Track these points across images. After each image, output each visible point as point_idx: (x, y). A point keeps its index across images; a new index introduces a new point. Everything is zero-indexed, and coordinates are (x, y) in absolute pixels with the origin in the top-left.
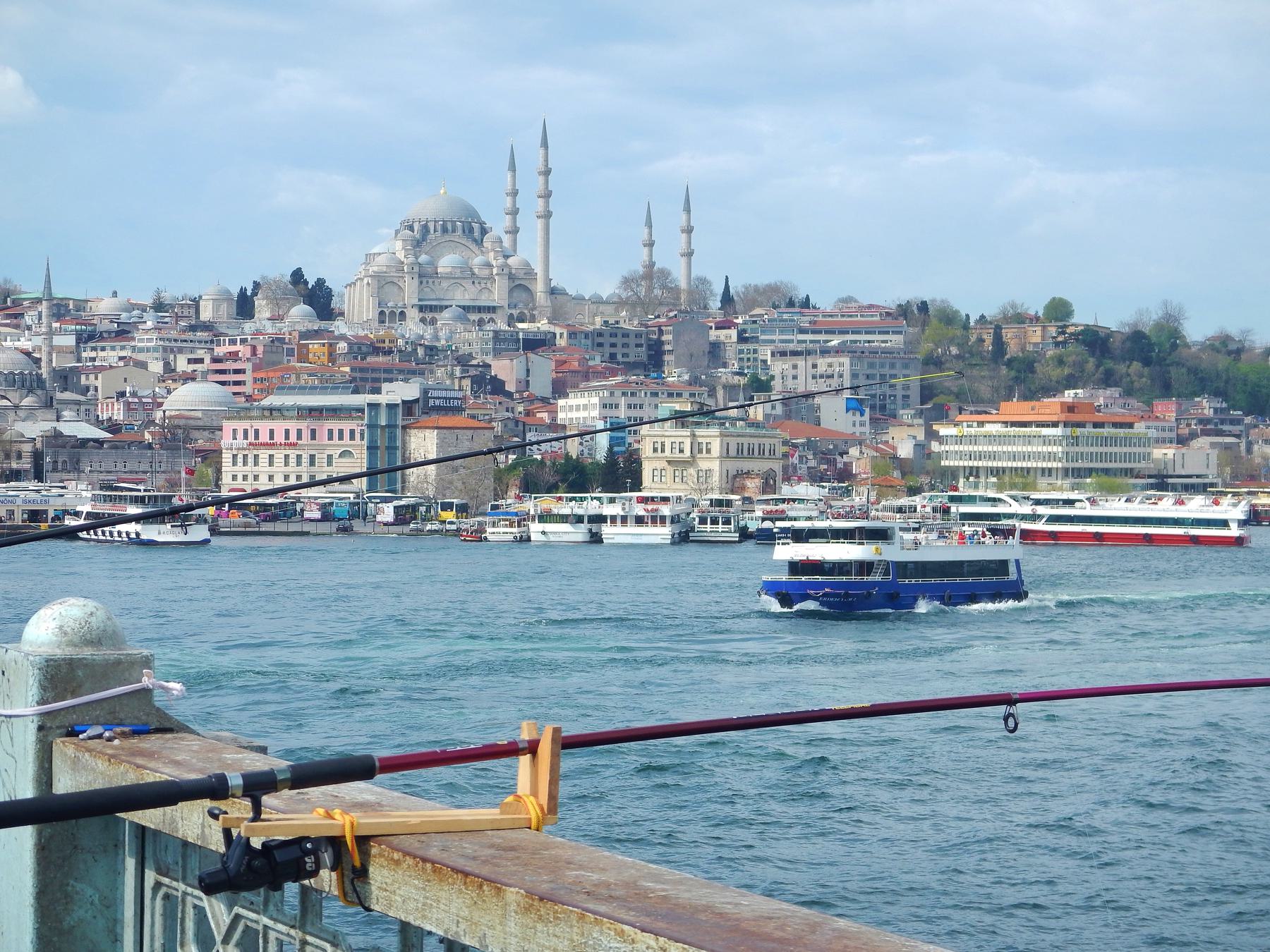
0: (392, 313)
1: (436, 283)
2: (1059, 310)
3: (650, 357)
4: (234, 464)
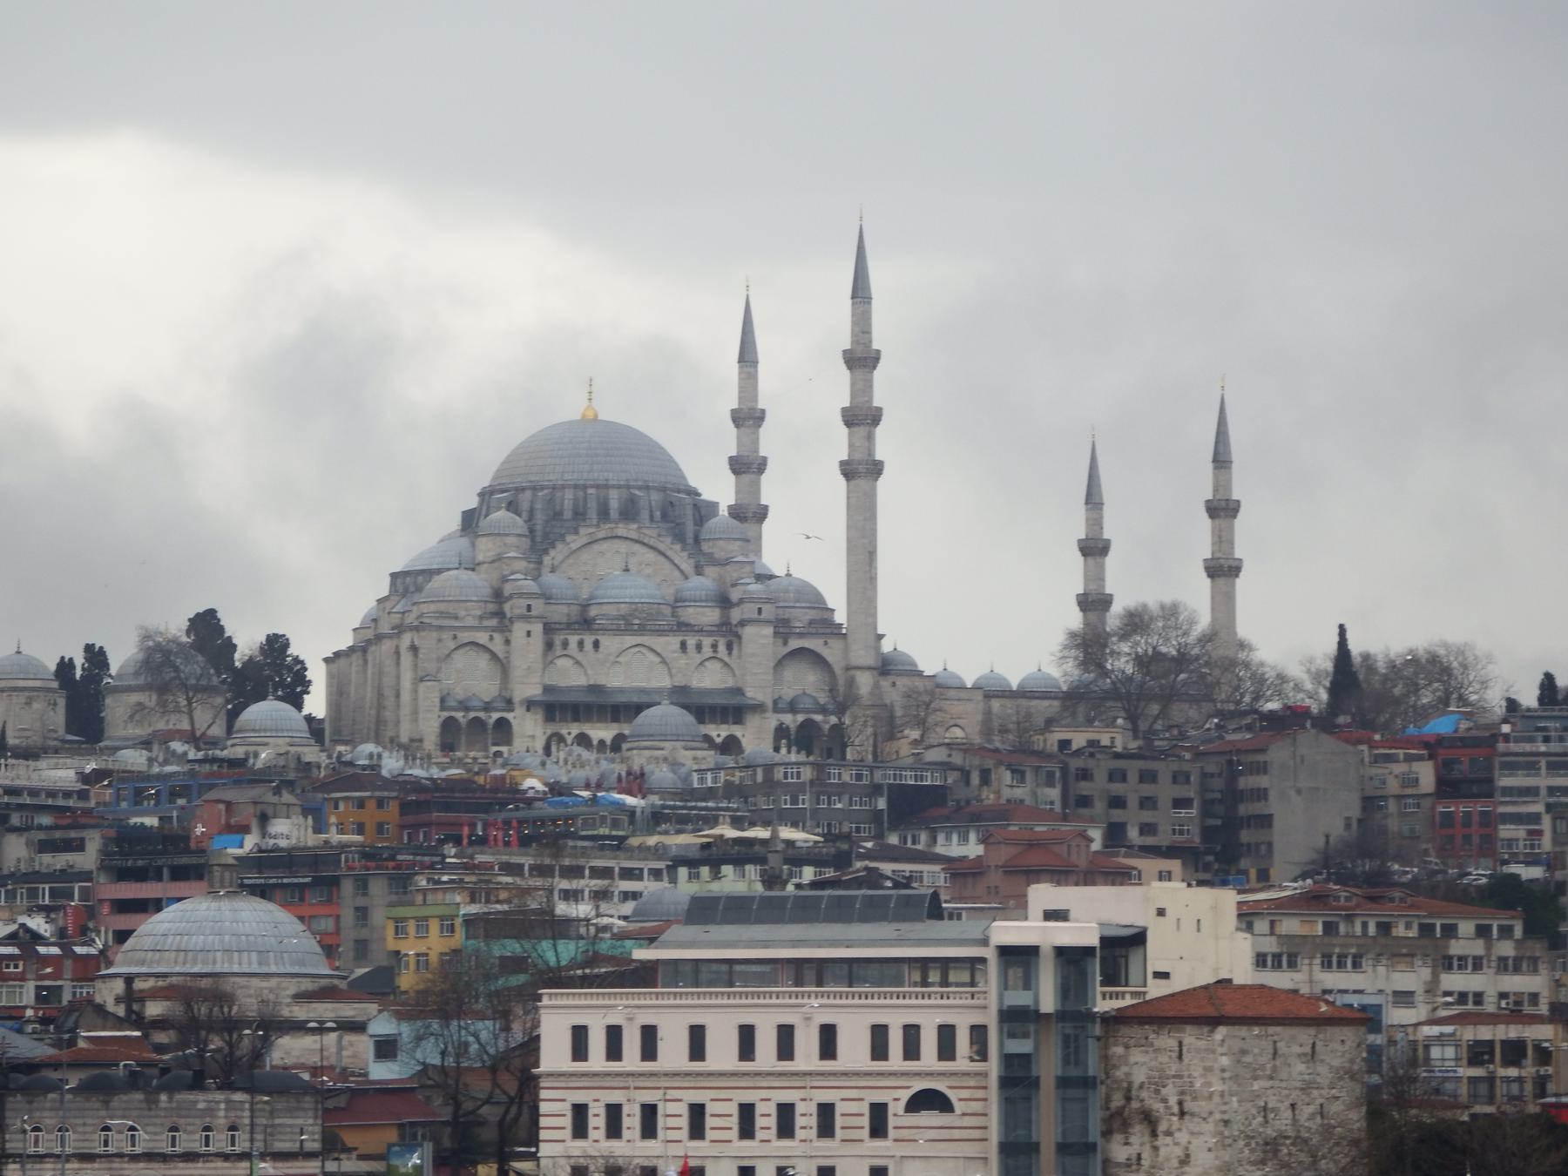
1: (588, 646)
3: (1207, 832)
4: (580, 1130)
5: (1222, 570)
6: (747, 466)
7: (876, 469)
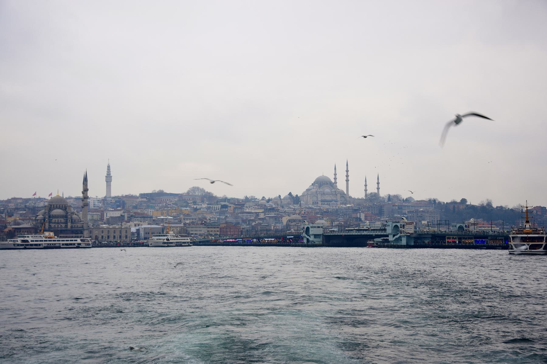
0: (315, 202)
2: (464, 201)
5: (378, 189)
6: (335, 179)
7: (349, 180)
